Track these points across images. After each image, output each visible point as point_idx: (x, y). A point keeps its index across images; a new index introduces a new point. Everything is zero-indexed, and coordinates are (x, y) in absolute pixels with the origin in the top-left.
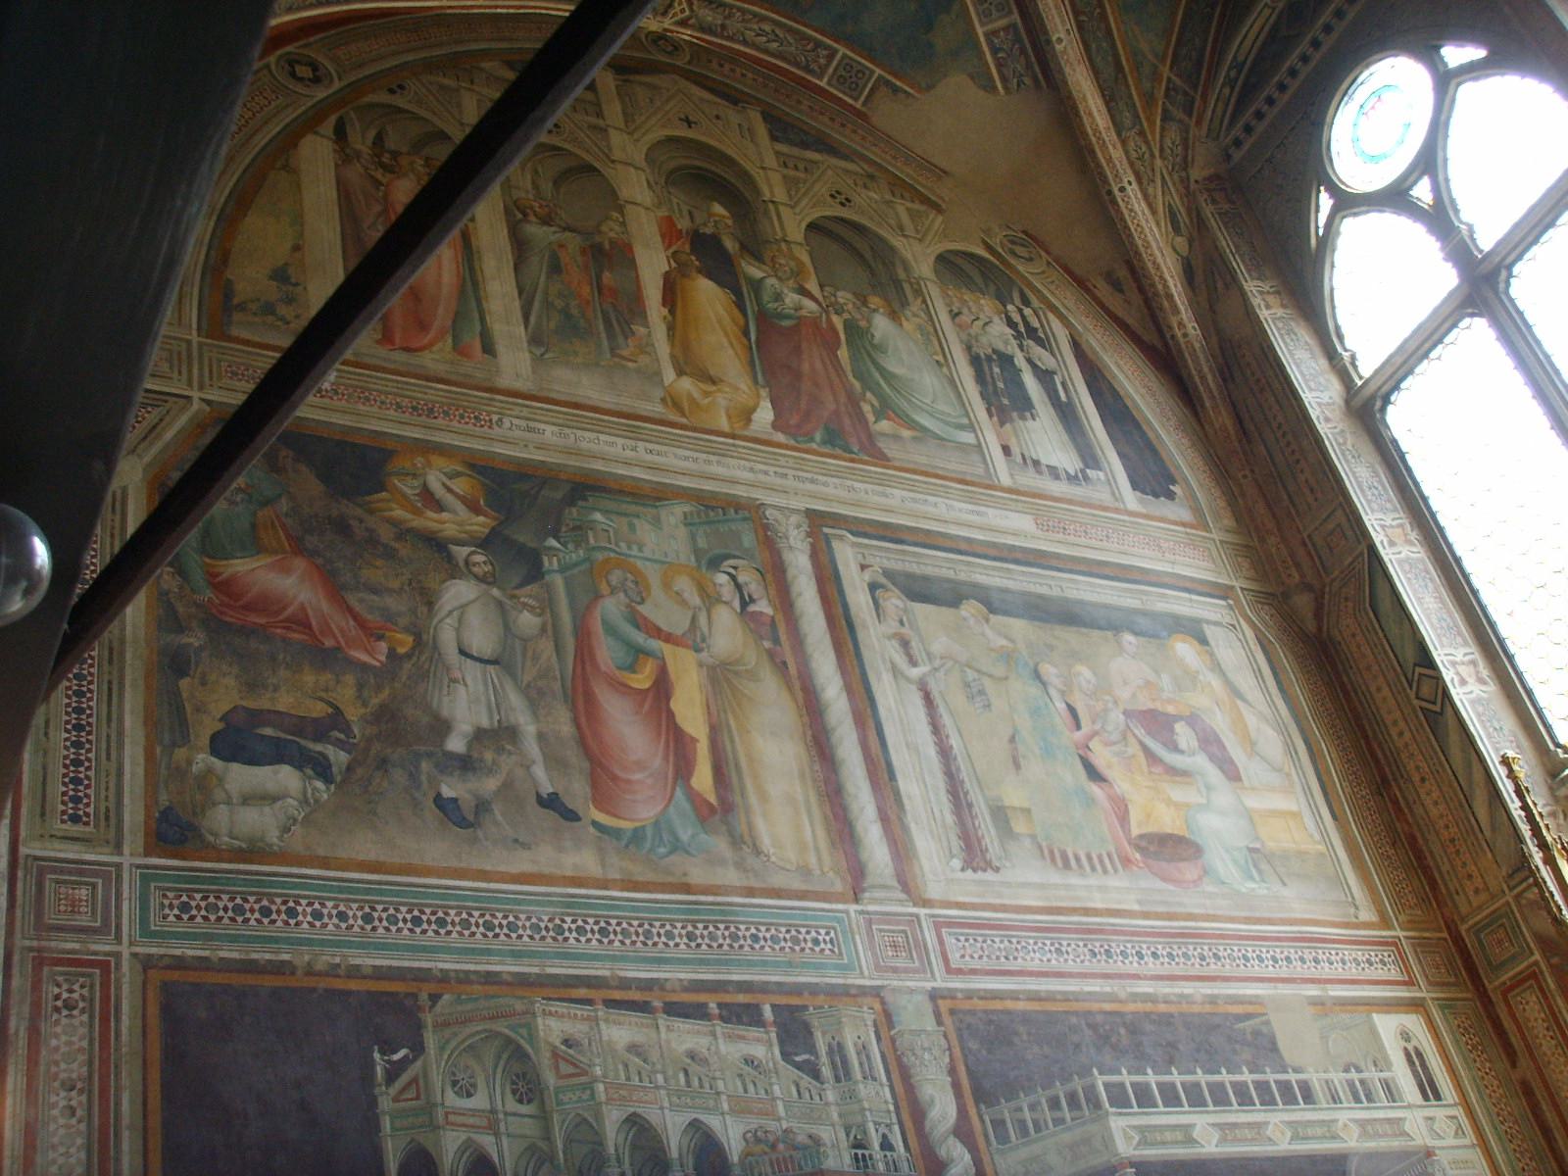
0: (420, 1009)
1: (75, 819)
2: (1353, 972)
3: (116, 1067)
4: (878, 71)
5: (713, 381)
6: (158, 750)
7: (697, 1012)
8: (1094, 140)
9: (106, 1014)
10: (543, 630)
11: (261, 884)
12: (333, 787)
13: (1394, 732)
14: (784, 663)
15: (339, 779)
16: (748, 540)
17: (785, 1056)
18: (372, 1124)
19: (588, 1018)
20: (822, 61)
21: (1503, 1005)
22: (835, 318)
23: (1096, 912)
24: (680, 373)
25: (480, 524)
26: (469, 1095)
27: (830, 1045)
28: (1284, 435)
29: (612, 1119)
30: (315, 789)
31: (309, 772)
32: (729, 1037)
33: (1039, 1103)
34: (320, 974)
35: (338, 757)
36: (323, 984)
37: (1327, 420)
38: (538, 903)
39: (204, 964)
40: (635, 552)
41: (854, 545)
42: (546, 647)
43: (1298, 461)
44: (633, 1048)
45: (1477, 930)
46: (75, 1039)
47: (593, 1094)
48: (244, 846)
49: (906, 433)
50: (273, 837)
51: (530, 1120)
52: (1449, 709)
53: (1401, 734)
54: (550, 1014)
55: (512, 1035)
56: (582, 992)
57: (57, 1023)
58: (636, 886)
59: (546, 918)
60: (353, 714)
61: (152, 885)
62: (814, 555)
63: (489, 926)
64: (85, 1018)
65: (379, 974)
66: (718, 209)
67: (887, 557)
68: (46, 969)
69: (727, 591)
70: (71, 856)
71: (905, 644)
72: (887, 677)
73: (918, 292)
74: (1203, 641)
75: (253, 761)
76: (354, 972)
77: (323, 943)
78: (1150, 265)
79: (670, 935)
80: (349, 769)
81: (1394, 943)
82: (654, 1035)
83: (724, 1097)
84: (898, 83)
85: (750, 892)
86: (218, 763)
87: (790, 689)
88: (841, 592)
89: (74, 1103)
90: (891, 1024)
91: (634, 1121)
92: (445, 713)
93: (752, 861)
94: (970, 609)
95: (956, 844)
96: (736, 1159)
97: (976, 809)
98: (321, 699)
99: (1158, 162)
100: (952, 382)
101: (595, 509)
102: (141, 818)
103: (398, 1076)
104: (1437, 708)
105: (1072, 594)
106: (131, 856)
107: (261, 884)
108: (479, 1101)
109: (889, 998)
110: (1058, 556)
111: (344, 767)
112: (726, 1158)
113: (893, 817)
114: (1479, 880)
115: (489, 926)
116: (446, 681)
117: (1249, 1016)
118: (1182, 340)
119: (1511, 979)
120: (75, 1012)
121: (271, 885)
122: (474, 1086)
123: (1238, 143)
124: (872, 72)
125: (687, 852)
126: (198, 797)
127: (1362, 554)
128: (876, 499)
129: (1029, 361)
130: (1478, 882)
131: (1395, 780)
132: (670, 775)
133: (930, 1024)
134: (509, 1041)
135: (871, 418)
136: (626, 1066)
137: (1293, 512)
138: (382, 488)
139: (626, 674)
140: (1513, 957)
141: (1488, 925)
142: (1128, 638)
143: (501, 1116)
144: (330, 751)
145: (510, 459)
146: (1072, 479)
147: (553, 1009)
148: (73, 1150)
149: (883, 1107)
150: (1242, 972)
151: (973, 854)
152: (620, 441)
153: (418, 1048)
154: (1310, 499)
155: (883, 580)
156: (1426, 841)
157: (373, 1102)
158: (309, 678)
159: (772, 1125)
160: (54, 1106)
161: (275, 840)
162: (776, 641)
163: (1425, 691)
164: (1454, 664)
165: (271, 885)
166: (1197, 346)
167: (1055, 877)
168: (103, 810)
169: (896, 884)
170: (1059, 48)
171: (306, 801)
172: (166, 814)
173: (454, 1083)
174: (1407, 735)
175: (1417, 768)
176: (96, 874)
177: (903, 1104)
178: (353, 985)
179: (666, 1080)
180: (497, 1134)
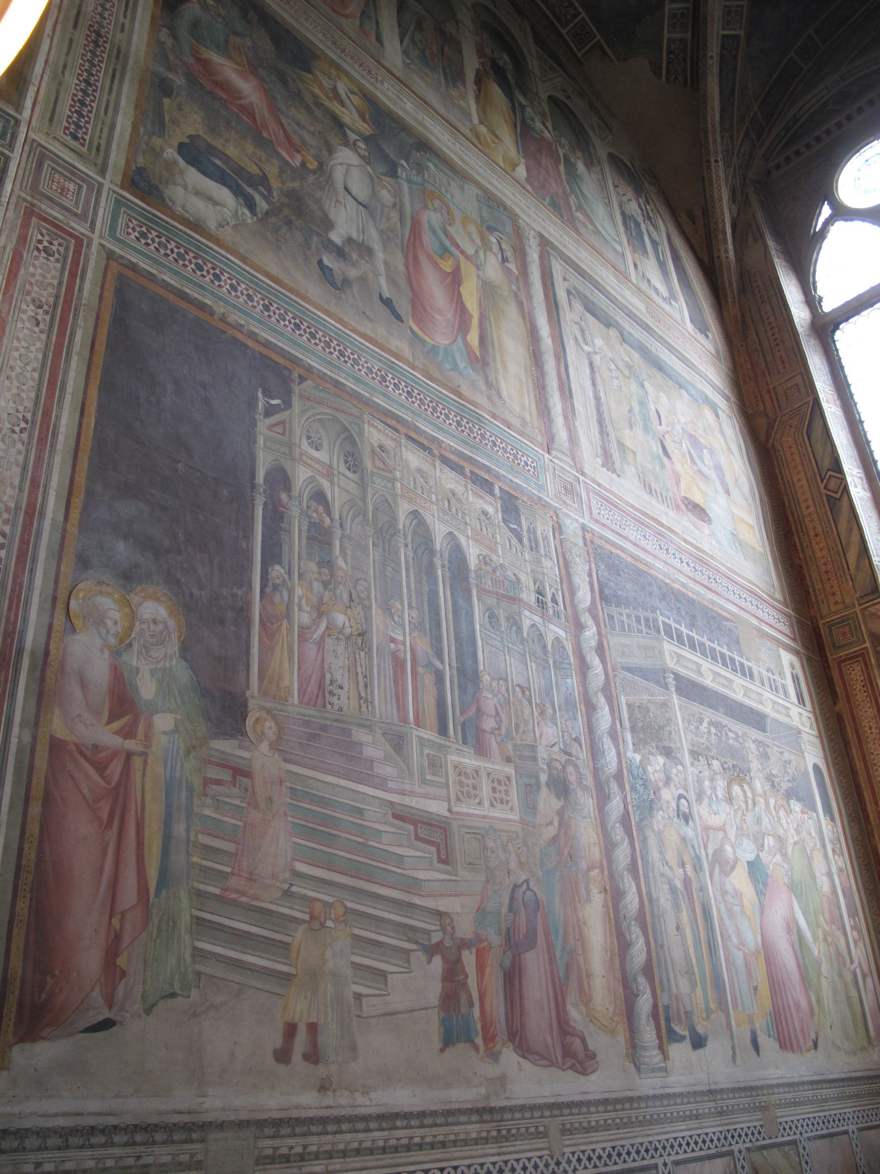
0: (292, 381)
1: (75, 137)
2: (772, 622)
3: (76, 310)
4: (599, 37)
5: (497, 137)
6: (142, 130)
7: (457, 469)
8: (710, 126)
9: (75, 272)
10: (394, 205)
11: (199, 248)
12: (255, 218)
13: (803, 506)
14: (522, 303)
15: (260, 216)
16: (509, 228)
17: (504, 521)
18: (252, 439)
19: (395, 440)
20: (569, 17)
21: (836, 670)
22: (559, 149)
23: (662, 525)
24: (481, 122)
25: (365, 128)
26: (317, 449)
27: (529, 528)
28: (772, 329)
29: (403, 508)
30: (243, 213)
31: (241, 201)
32: (476, 494)
33: (631, 616)
34: (229, 324)
35: (262, 205)
36: (230, 332)
37: (802, 326)
38: (372, 356)
39: (151, 277)
40: (449, 196)
41: (561, 264)
42: (395, 216)
43: (777, 345)
44: (419, 471)
45: (830, 625)
46: (49, 276)
47: (393, 487)
48: (191, 219)
49: (590, 226)
50: (212, 225)
51: (354, 485)
52: (845, 497)
53: (808, 507)
54: (373, 425)
55: (347, 425)
56: (393, 423)
57: (36, 258)
58: (431, 378)
59: (377, 368)
60: (274, 183)
61: (123, 209)
62: (541, 257)
63: (342, 354)
64: (59, 266)
65: (267, 344)
66: (506, 57)
67: (576, 281)
68: (34, 220)
69: (495, 248)
70: (67, 158)
71: (582, 331)
72: (572, 342)
73: (599, 163)
74: (717, 416)
75: (204, 173)
76: (253, 336)
77: (234, 306)
78: (718, 211)
79: (447, 416)
80: (267, 213)
81: (788, 616)
82: (433, 470)
83: (469, 528)
84: (608, 50)
85: (494, 416)
86: (181, 162)
87: (524, 317)
88: (553, 284)
89: (39, 318)
90: (561, 533)
91: (415, 514)
92: (332, 216)
93: (495, 399)
94: (613, 332)
95: (600, 451)
96: (473, 569)
97: (610, 438)
98: (257, 165)
99: (735, 158)
100: (612, 217)
101: (430, 161)
102: (122, 163)
103: (273, 414)
104: (837, 496)
105: (662, 356)
106: (111, 182)
107: (199, 248)
108: (322, 455)
109: (561, 516)
110: (656, 332)
111: (264, 211)
113: (570, 417)
114: (840, 596)
115: (342, 354)
116: (334, 199)
117: (728, 620)
118: (724, 260)
119: (846, 655)
120: (52, 259)
121: (206, 253)
122: (321, 445)
123: (778, 167)
124: (595, 37)
125: (461, 374)
126: (165, 173)
127: (808, 402)
128: (573, 248)
129: (647, 230)
130: (838, 598)
131: (797, 532)
132: (456, 326)
133: (581, 543)
134: (346, 429)
135: (574, 208)
136: (415, 480)
137: (766, 372)
138: (309, 71)
139: (438, 258)
140: (851, 643)
141: (838, 623)
142: (684, 393)
143: (336, 472)
144: (257, 197)
145: (387, 107)
146: (664, 299)
147: (375, 424)
148: (33, 349)
149: (554, 577)
150: (725, 594)
151: (608, 462)
152: (447, 136)
153: (288, 405)
154: (780, 367)
155: (573, 291)
156: (809, 570)
157: (254, 423)
158: (250, 148)
159: (495, 558)
160: (25, 312)
161: (213, 228)
162: (519, 289)
163: (832, 485)
164: (852, 475)
165: (206, 253)
166: (732, 266)
167: (645, 496)
168: (95, 144)
169: (568, 453)
170: (710, 62)
171: (237, 217)
172: (140, 171)
173: (309, 438)
174: (812, 508)
175: (814, 528)
176: (84, 181)
177: (564, 581)
178: (250, 343)
179: (437, 499)
180: (332, 483)
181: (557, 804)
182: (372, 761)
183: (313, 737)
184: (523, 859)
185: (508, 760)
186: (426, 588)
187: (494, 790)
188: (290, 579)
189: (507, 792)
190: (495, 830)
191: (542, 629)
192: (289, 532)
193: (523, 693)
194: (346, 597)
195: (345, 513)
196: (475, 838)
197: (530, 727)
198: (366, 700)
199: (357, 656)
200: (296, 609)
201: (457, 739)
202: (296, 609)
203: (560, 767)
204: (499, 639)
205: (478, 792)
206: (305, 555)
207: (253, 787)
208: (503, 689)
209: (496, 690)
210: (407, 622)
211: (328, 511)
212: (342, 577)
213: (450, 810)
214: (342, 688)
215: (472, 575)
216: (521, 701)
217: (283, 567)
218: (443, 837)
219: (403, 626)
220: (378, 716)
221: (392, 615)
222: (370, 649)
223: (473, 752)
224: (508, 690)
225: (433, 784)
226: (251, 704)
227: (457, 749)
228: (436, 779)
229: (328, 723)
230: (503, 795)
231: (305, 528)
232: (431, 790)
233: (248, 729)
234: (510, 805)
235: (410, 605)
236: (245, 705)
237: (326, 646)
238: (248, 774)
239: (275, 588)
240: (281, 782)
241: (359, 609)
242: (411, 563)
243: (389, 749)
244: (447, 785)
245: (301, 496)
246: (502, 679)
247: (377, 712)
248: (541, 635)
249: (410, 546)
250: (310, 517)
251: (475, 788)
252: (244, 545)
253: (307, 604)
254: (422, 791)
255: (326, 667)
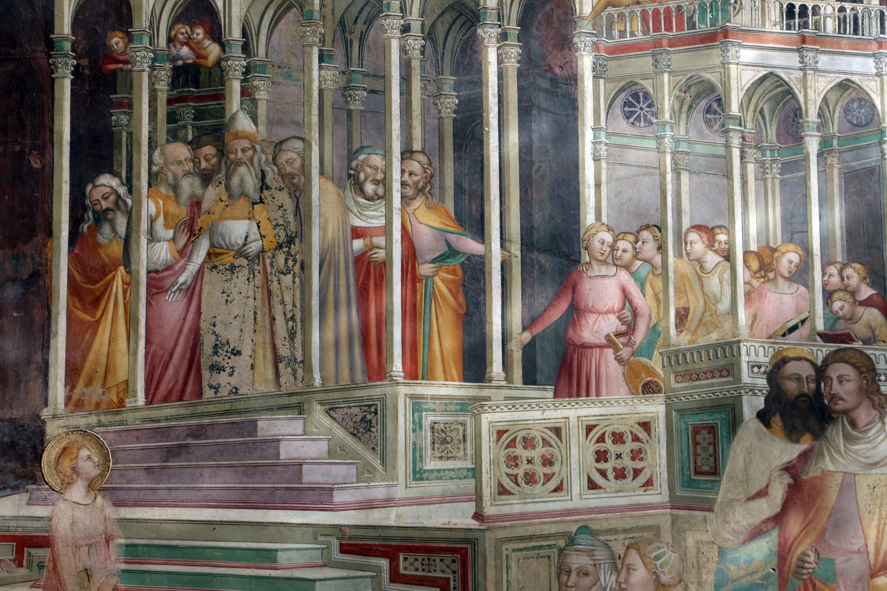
112: (572, 11)
181: (791, 451)
182: (301, 465)
183: (172, 453)
184: (665, 579)
185: (650, 388)
186: (450, 103)
187: (601, 456)
188: (130, 191)
189: (636, 455)
190: (593, 533)
191: (793, 78)
192: (129, 106)
193: (711, 243)
194: (251, 184)
195: (255, 20)
196: (538, 557)
197: (724, 305)
198: (292, 361)
199: (275, 286)
200: (144, 241)
201: (508, 378)
202: (144, 241)
203: (806, 370)
204: (652, 144)
205: (556, 468)
206: (162, 135)
207: (54, 560)
208: (649, 249)
209: (627, 256)
210: (396, 186)
211: (216, 33)
212: (244, 151)
213: (478, 516)
214: (239, 353)
215: (586, 27)
216: (700, 261)
217: (115, 174)
218: (456, 567)
219: (386, 196)
220: (318, 381)
221: (359, 188)
222: (304, 267)
223: (550, 394)
224: (661, 248)
225: (439, 474)
226: (52, 429)
227: (506, 398)
228: (451, 464)
229: (207, 421)
230: (627, 462)
231: (163, 87)
232: (435, 488)
233: (45, 470)
234: (642, 478)
235: (407, 153)
236: (42, 433)
237: (206, 288)
238: (44, 542)
239: (101, 217)
240: (108, 541)
241: (284, 198)
242: (416, 64)
243: (339, 432)
244: (475, 473)
245: (154, 24)
246: (647, 227)
247: (317, 376)
248: (790, 92)
249: (416, 27)
250: (174, 59)
251: (547, 462)
252: (37, 165)
253: (166, 226)
254: (413, 493)
255: (203, 325)
